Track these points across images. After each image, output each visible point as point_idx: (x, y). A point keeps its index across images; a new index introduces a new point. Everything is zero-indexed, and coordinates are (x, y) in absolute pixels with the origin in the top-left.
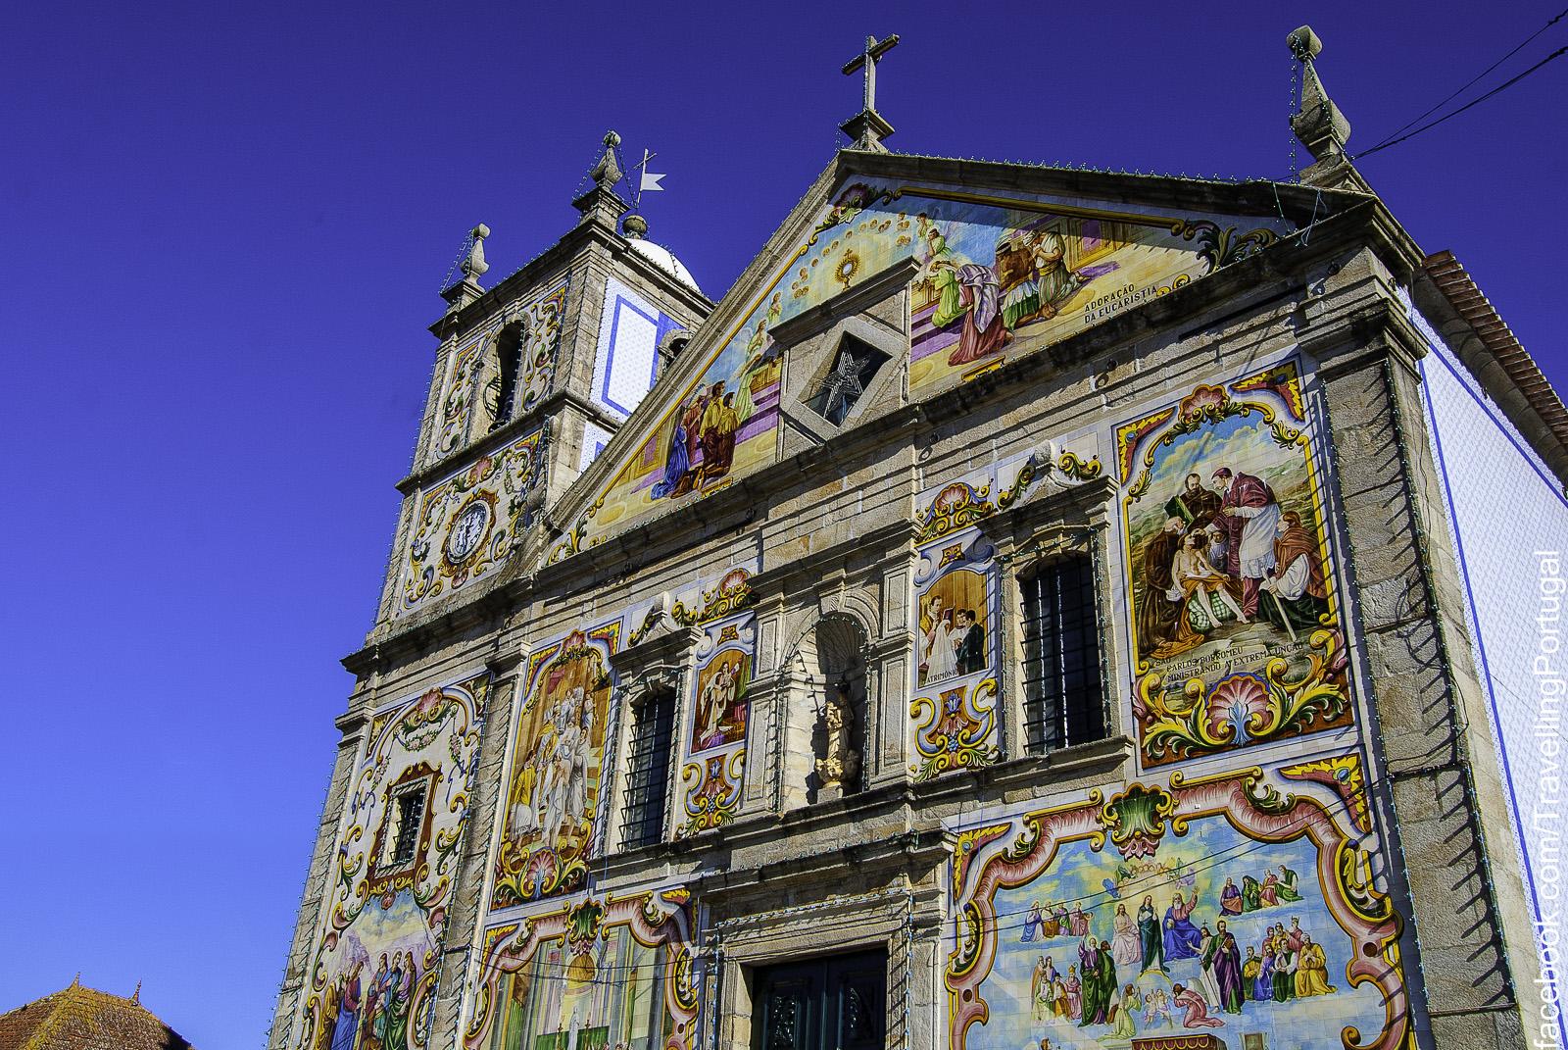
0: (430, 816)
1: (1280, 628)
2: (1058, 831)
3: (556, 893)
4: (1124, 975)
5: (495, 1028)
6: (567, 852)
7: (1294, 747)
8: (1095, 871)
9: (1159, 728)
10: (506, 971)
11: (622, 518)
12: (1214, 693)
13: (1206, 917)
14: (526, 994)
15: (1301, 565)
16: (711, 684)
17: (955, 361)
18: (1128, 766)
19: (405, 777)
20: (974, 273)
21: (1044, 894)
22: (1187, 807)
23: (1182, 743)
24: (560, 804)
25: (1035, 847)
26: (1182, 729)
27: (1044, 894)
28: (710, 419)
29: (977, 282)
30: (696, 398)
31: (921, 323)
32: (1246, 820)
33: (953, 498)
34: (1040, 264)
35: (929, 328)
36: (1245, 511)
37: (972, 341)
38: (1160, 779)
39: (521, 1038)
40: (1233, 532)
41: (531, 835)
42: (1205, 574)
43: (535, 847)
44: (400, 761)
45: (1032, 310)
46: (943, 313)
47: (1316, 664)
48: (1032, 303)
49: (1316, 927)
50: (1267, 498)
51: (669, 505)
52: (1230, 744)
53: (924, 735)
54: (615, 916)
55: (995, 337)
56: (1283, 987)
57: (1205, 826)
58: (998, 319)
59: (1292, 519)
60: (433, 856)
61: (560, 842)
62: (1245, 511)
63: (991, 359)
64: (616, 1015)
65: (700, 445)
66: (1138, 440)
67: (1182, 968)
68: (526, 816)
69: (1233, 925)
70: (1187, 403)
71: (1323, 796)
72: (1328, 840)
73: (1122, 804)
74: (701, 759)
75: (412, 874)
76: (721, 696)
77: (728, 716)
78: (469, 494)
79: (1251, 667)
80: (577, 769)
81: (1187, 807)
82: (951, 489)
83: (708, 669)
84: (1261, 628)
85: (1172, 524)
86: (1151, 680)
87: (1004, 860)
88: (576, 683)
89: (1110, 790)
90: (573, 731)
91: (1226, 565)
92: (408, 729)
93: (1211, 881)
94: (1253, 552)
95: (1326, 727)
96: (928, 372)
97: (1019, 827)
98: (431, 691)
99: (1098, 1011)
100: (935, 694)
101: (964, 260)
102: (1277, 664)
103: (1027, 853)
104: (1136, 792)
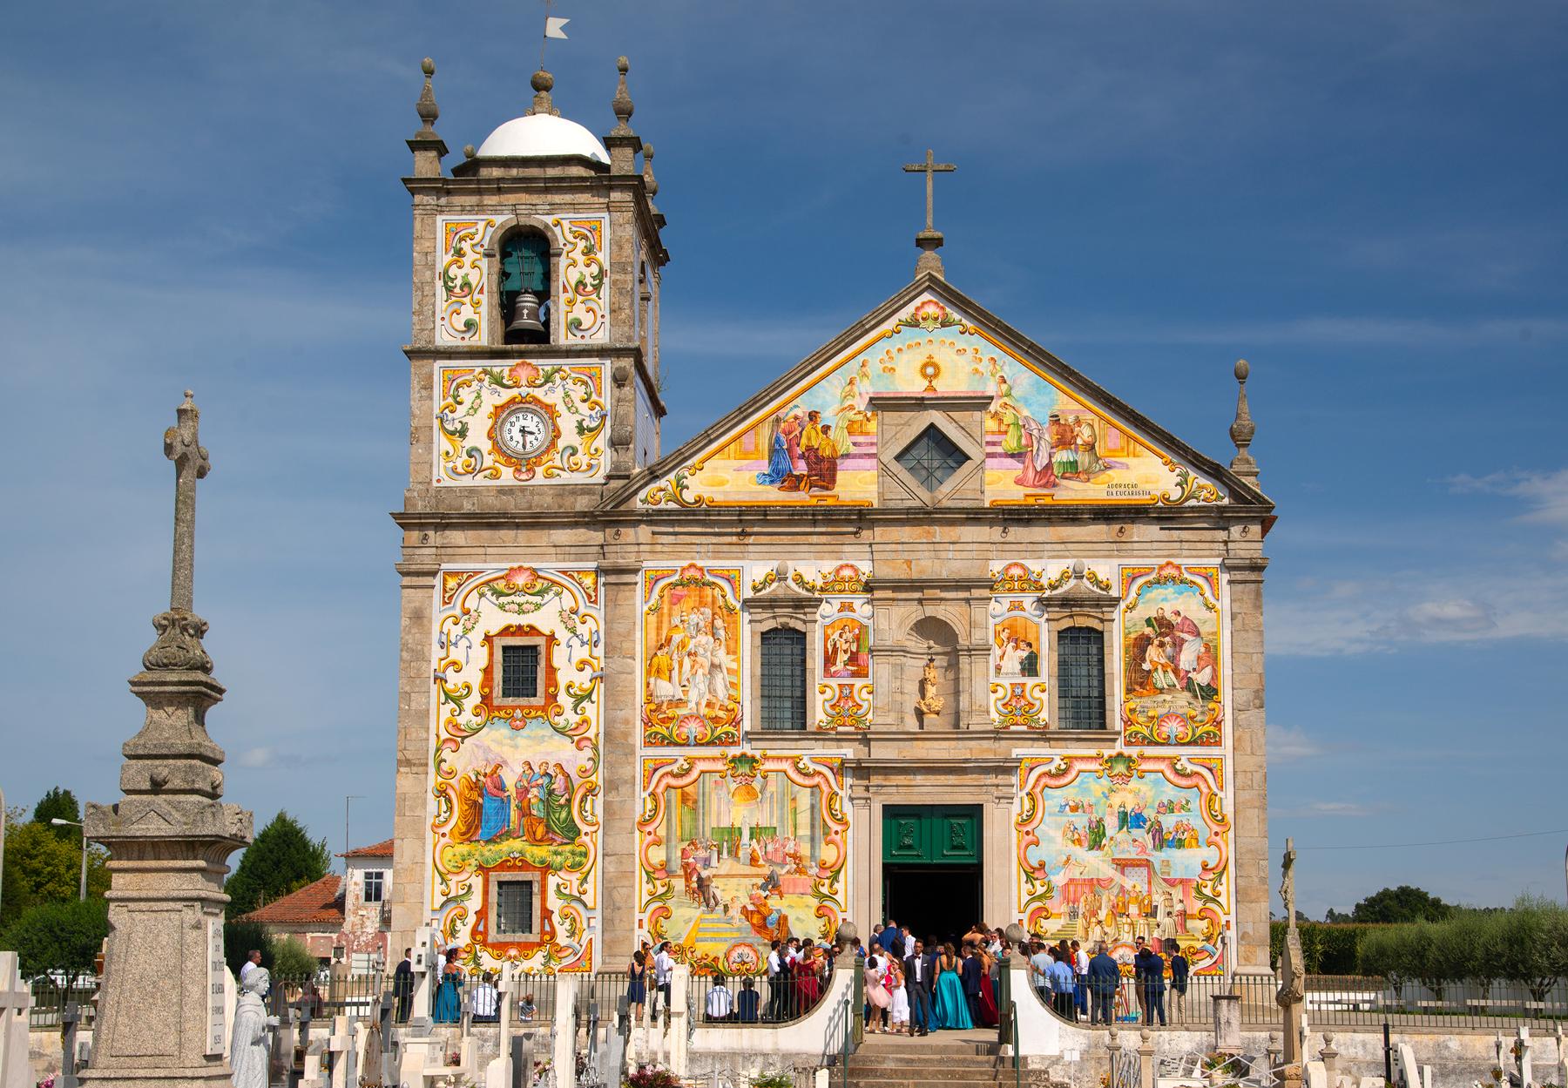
0: (552, 671)
2: (1078, 766)
5: (669, 820)
6: (715, 720)
10: (669, 787)
11: (727, 488)
14: (696, 802)
15: (1208, 670)
16: (836, 636)
17: (1018, 482)
18: (1118, 743)
19: (506, 631)
20: (1034, 426)
21: (1071, 794)
23: (1144, 738)
24: (703, 687)
25: (1064, 773)
26: (1146, 732)
27: (1071, 794)
28: (809, 439)
29: (1035, 432)
30: (792, 414)
31: (994, 444)
32: (1171, 776)
34: (1079, 441)
35: (999, 450)
37: (1031, 474)
38: (1133, 751)
39: (696, 828)
40: (1178, 644)
42: (1163, 661)
43: (683, 711)
44: (493, 618)
45: (1072, 470)
46: (1010, 443)
48: (1074, 464)
50: (1198, 634)
52: (1166, 743)
53: (999, 704)
54: (769, 765)
55: (1046, 475)
56: (1180, 844)
57: (1153, 776)
58: (1049, 466)
59: (1207, 646)
60: (564, 700)
61: (704, 711)
63: (1045, 491)
64: (782, 819)
65: (802, 456)
67: (1137, 833)
68: (665, 689)
69: (1161, 818)
70: (1161, 568)
72: (1205, 790)
74: (834, 682)
75: (544, 709)
76: (845, 647)
77: (853, 658)
78: (514, 392)
79: (1180, 711)
80: (713, 665)
82: (1016, 565)
83: (832, 625)
84: (1187, 695)
85: (1148, 631)
86: (1132, 705)
87: (1049, 774)
88: (702, 603)
89: (1107, 753)
90: (705, 639)
91: (1173, 659)
92: (499, 594)
94: (1187, 659)
95: (1210, 744)
96: (1002, 484)
97: (1057, 761)
98: (520, 568)
100: (1006, 682)
101: (1026, 413)
102: (1193, 713)
104: (1120, 755)
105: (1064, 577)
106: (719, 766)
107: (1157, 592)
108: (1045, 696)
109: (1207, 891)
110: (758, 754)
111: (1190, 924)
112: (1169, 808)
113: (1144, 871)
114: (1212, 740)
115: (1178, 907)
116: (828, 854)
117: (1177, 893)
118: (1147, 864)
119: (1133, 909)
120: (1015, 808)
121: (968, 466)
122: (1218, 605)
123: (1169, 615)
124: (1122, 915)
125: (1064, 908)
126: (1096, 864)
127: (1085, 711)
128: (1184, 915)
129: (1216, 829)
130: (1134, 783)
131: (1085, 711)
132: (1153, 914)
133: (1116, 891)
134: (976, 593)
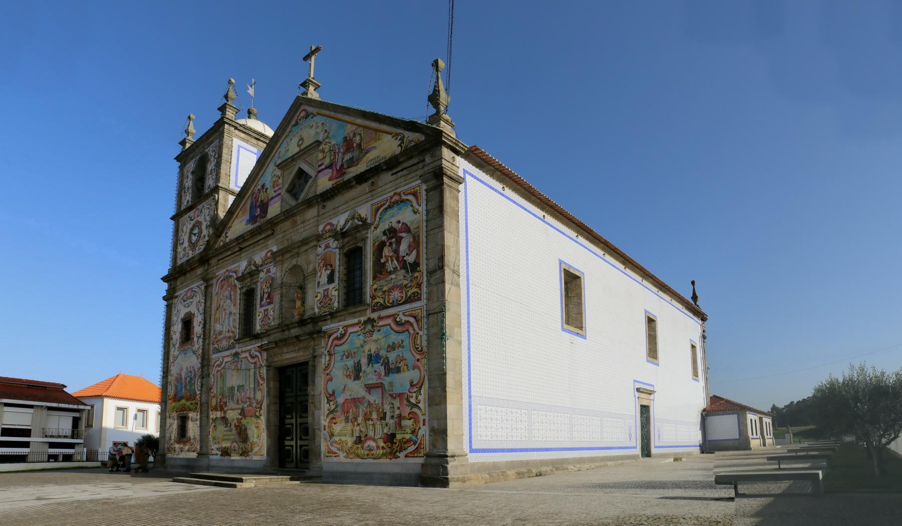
1: (407, 272)
2: (350, 330)
3: (228, 349)
4: (363, 368)
6: (230, 337)
7: (407, 306)
8: (358, 340)
9: (376, 301)
12: (390, 291)
13: (383, 353)
15: (414, 252)
18: (369, 311)
21: (345, 347)
22: (381, 323)
23: (381, 305)
26: (381, 301)
33: (328, 227)
36: (403, 235)
38: (375, 315)
41: (220, 333)
47: (415, 282)
49: (408, 355)
51: (250, 227)
54: (243, 355)
56: (398, 370)
57: (385, 328)
59: (414, 238)
61: (228, 335)
62: (403, 235)
66: (377, 210)
69: (389, 355)
70: (391, 198)
71: (412, 320)
72: (412, 332)
73: (365, 323)
74: (262, 310)
81: (381, 323)
84: (403, 271)
85: (384, 238)
86: (375, 287)
87: (337, 338)
89: (363, 319)
90: (228, 301)
91: (396, 251)
93: (384, 343)
94: (404, 247)
96: (324, 183)
97: (341, 330)
99: (357, 378)
100: (321, 290)
102: (406, 282)
103: (343, 336)
104: (369, 319)
105: (347, 222)
106: (229, 359)
107: (391, 212)
108: (336, 293)
109: (413, 400)
110: (239, 350)
111: (404, 423)
112: (392, 348)
113: (380, 390)
114: (416, 297)
115: (397, 412)
116: (259, 396)
117: (397, 403)
118: (381, 386)
119: (374, 416)
120: (323, 360)
121: (311, 180)
122: (420, 209)
123: (395, 225)
124: (369, 419)
125: (343, 418)
126: (357, 389)
127: (353, 296)
128: (400, 417)
129: (418, 357)
130: (376, 336)
131: (353, 296)
132: (384, 418)
133: (366, 404)
134: (312, 244)
